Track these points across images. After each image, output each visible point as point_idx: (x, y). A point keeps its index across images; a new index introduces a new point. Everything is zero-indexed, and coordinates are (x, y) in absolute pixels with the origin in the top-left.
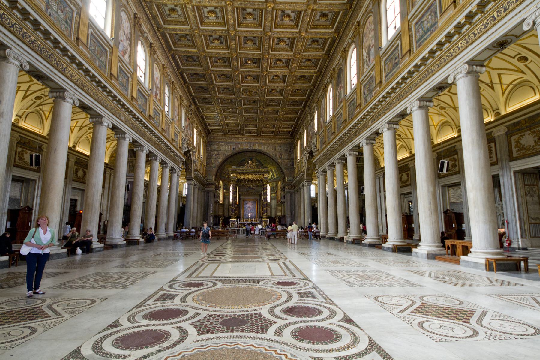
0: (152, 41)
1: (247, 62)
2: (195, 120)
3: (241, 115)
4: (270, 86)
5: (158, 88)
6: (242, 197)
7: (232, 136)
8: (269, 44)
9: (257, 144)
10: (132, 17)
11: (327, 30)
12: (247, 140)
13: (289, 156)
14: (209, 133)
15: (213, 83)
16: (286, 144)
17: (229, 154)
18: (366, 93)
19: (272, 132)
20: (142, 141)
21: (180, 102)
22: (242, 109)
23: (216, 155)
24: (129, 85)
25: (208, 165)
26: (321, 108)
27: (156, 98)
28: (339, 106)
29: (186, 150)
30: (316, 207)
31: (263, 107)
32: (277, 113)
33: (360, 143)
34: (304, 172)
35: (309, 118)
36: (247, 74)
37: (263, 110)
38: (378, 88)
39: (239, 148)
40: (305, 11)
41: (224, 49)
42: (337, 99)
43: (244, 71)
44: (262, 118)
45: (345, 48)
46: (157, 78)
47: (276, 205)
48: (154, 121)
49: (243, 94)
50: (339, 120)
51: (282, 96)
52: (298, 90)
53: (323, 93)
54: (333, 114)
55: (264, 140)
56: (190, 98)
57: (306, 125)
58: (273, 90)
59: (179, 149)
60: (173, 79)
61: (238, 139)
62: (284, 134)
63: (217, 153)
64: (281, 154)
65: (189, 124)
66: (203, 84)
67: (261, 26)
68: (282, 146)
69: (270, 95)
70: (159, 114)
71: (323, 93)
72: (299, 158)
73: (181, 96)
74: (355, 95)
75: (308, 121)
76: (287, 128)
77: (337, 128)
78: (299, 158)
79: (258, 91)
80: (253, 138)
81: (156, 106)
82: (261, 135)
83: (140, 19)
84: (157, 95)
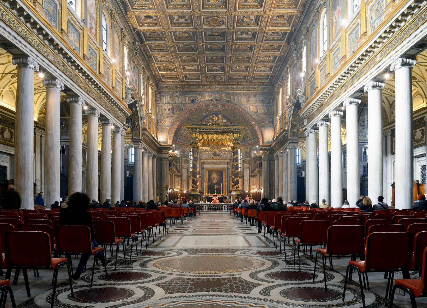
2: (141, 62)
3: (202, 54)
4: (241, 12)
5: (93, 18)
6: (205, 166)
9: (224, 94)
12: (210, 88)
13: (268, 110)
14: (160, 81)
15: (164, 12)
16: (263, 94)
18: (374, 17)
19: (245, 77)
20: (76, 90)
21: (122, 38)
22: (203, 45)
23: (169, 110)
24: (58, 14)
26: (312, 41)
27: (91, 32)
28: (336, 37)
29: (131, 102)
30: (303, 176)
31: (232, 42)
33: (364, 86)
35: (294, 56)
37: (232, 46)
38: (390, 9)
42: (334, 28)
44: (231, 57)
46: (91, 5)
47: (250, 176)
48: (89, 62)
50: (336, 56)
51: (258, 25)
52: (279, 16)
53: (315, 20)
54: (328, 48)
55: (233, 88)
56: (134, 32)
58: (245, 17)
59: (121, 100)
61: (198, 88)
62: (261, 79)
64: (256, 107)
65: (134, 68)
66: (151, 13)
68: (258, 96)
69: (241, 25)
70: (96, 54)
71: (315, 20)
72: (281, 112)
73: (122, 29)
74: (359, 20)
75: (294, 61)
76: (264, 71)
77: (333, 68)
81: (91, 43)
82: (229, 82)
84: (93, 28)
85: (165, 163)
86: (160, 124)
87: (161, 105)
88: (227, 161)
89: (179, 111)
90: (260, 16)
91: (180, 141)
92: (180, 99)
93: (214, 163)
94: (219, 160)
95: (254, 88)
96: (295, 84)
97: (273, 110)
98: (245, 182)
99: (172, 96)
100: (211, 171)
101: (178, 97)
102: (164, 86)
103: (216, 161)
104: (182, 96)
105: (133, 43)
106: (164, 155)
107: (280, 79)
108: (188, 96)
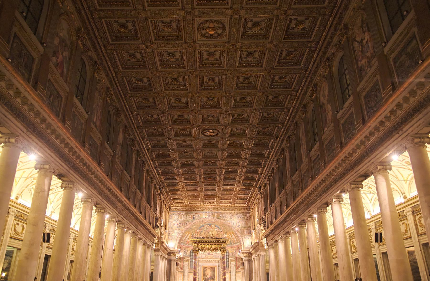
6: (201, 264)
9: (215, 214)
13: (247, 224)
16: (243, 213)
23: (177, 224)
47: (236, 272)
55: (222, 209)
61: (198, 209)
64: (238, 222)
68: (239, 214)
85: (173, 263)
86: (170, 234)
87: (172, 221)
88: (218, 260)
89: (185, 225)
91: (183, 244)
92: (185, 217)
93: (208, 261)
94: (212, 258)
95: (237, 209)
97: (250, 224)
98: (232, 276)
99: (180, 215)
100: (206, 268)
101: (184, 215)
102: (174, 208)
103: (210, 259)
104: (186, 215)
106: (172, 258)
108: (191, 215)
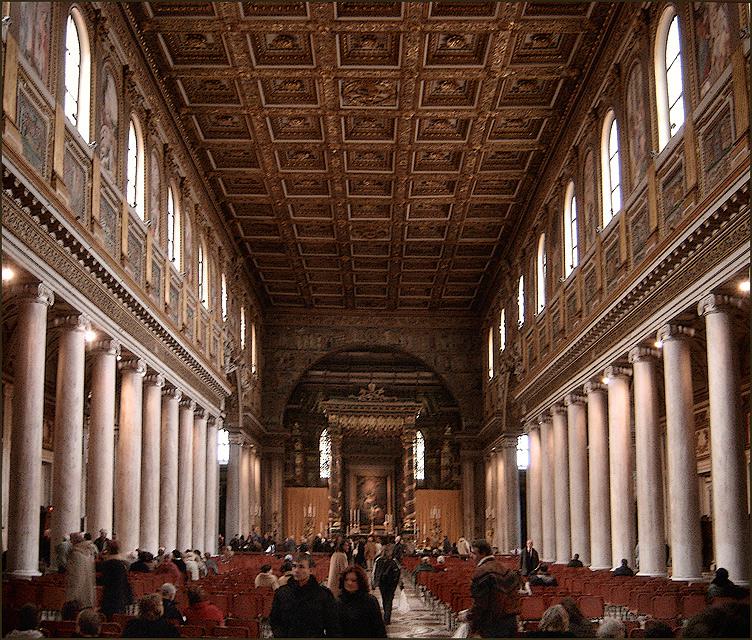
0: (183, 175)
1: (361, 183)
2: (243, 288)
6: (351, 467)
7: (323, 311)
8: (410, 160)
10: (161, 151)
11: (525, 141)
15: (288, 218)
17: (317, 357)
19: (425, 303)
23: (285, 361)
25: (268, 388)
31: (400, 255)
32: (434, 265)
34: (500, 413)
35: (507, 282)
36: (360, 202)
39: (341, 340)
40: (476, 120)
41: (316, 167)
43: (356, 199)
44: (399, 276)
45: (560, 179)
49: (354, 236)
57: (504, 298)
60: (210, 224)
63: (288, 354)
66: (268, 219)
67: (390, 136)
69: (414, 236)
72: (491, 374)
73: (220, 248)
78: (491, 374)
79: (386, 230)
80: (377, 315)
83: (172, 149)
90: (454, 182)
96: (510, 332)
105: (232, 260)
107: (490, 312)
